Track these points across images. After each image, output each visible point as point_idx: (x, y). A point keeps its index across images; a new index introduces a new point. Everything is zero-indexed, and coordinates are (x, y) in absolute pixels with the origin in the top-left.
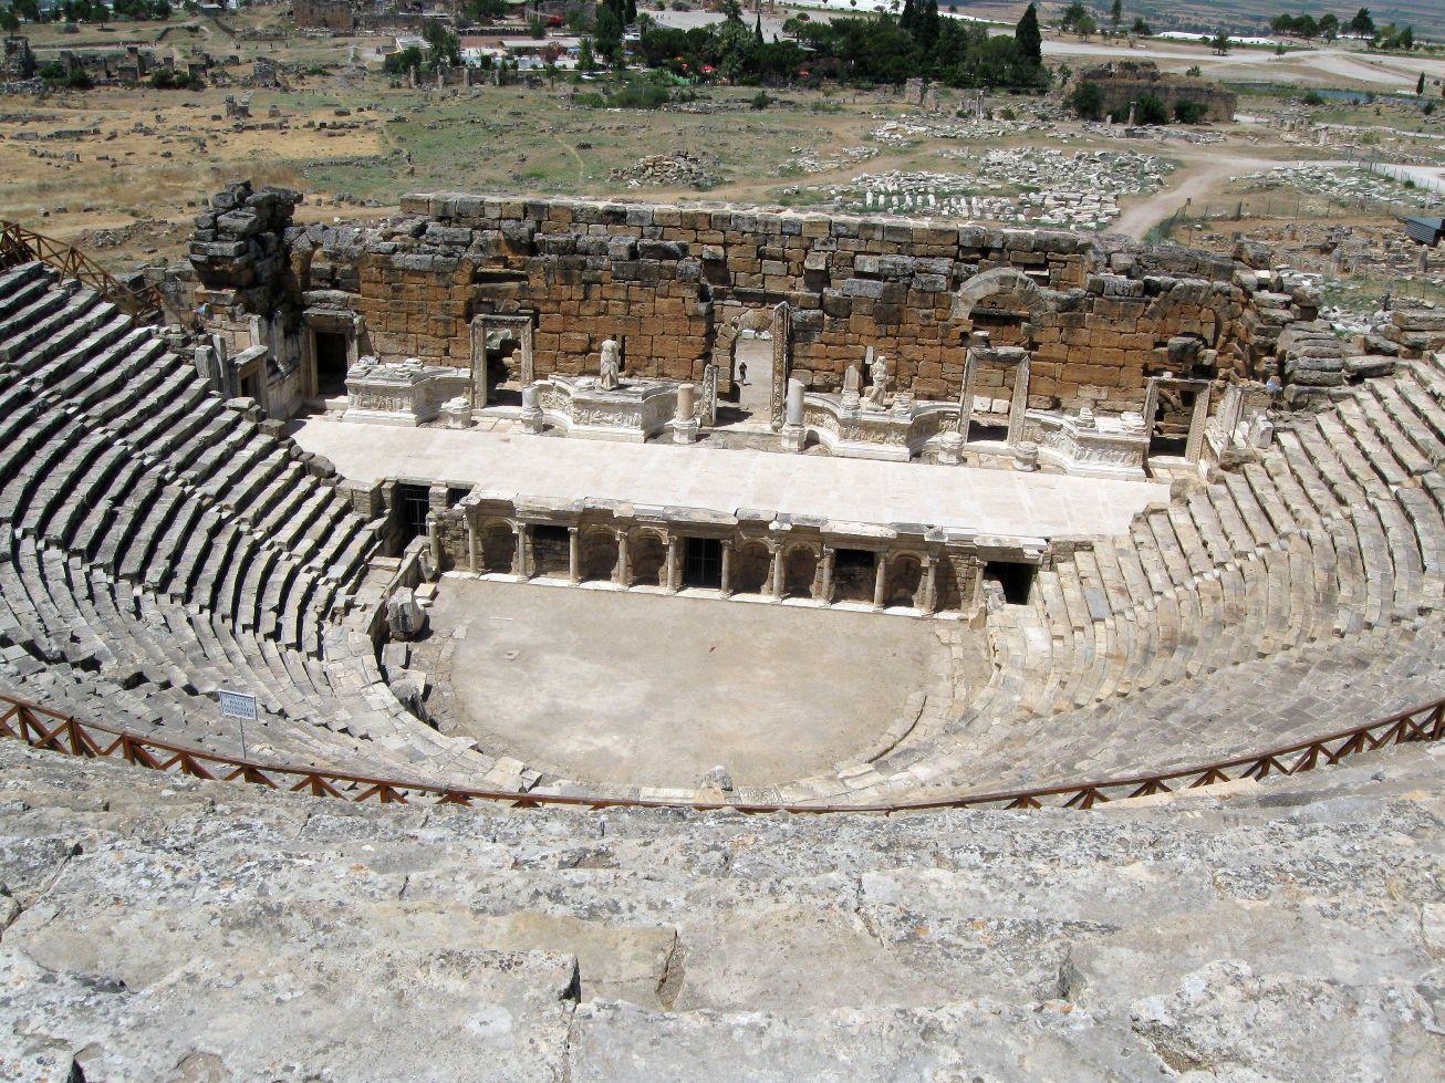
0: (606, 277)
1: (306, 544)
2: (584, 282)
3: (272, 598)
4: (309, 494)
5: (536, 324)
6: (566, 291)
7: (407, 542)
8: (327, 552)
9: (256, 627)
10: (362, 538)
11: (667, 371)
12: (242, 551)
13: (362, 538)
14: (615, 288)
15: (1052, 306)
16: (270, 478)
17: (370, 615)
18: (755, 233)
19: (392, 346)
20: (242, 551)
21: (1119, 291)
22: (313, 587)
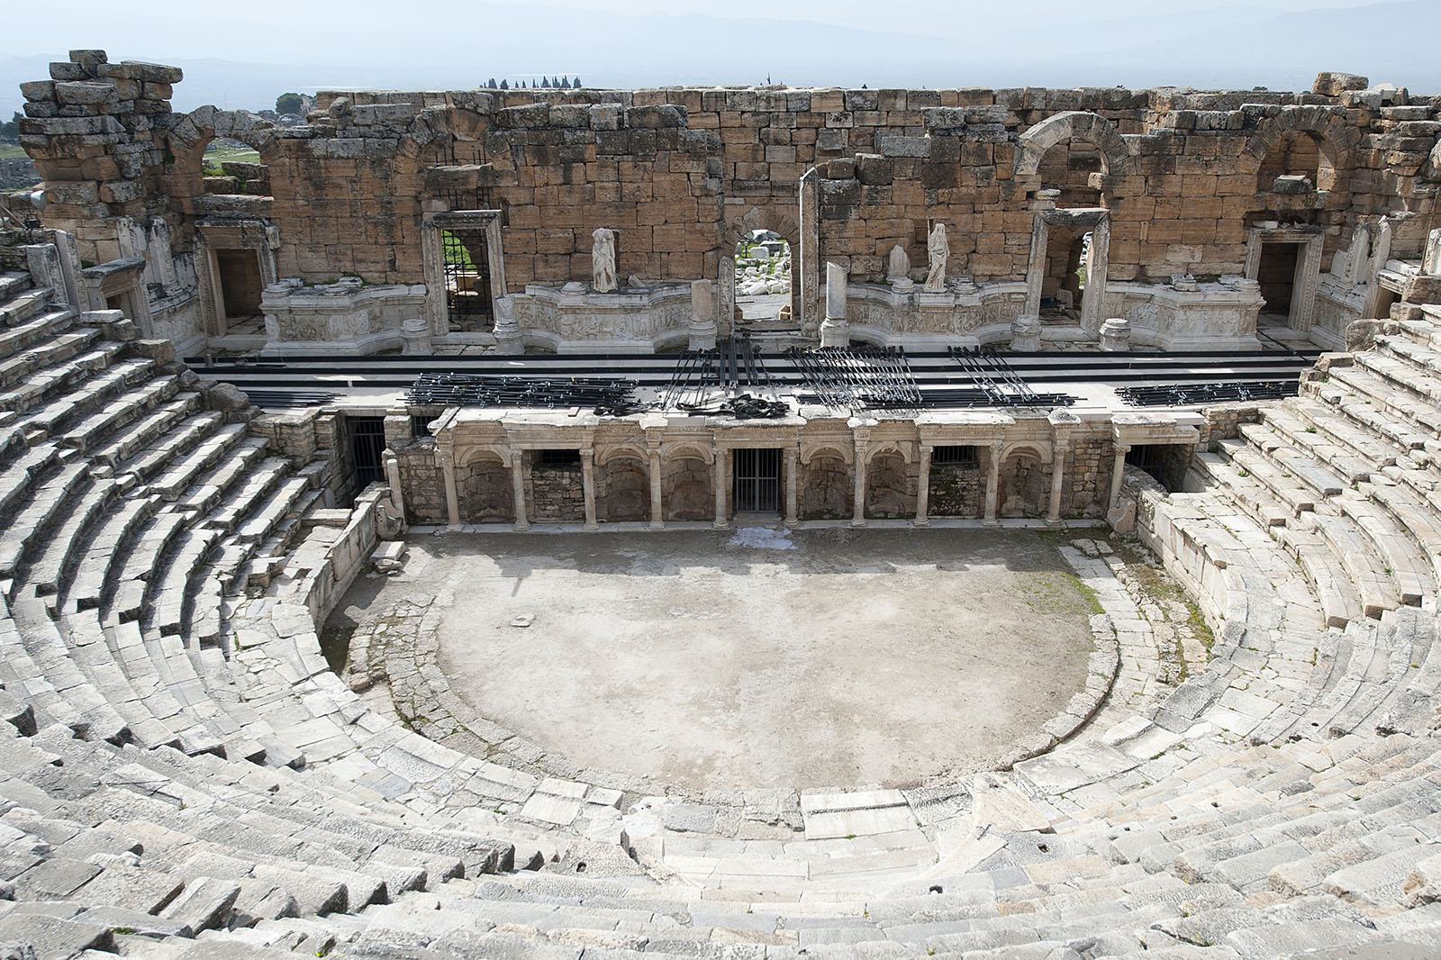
0: (590, 153)
1: (207, 491)
2: (563, 160)
3: (143, 560)
4: (207, 433)
5: (505, 221)
6: (541, 174)
7: (360, 488)
8: (241, 502)
9: (102, 603)
10: (293, 486)
11: (673, 270)
12: (92, 499)
13: (293, 486)
14: (602, 166)
15: (1134, 150)
16: (144, 410)
17: (308, 583)
18: (755, 113)
19: (317, 262)
20: (92, 499)
21: (1214, 123)
22: (212, 552)
